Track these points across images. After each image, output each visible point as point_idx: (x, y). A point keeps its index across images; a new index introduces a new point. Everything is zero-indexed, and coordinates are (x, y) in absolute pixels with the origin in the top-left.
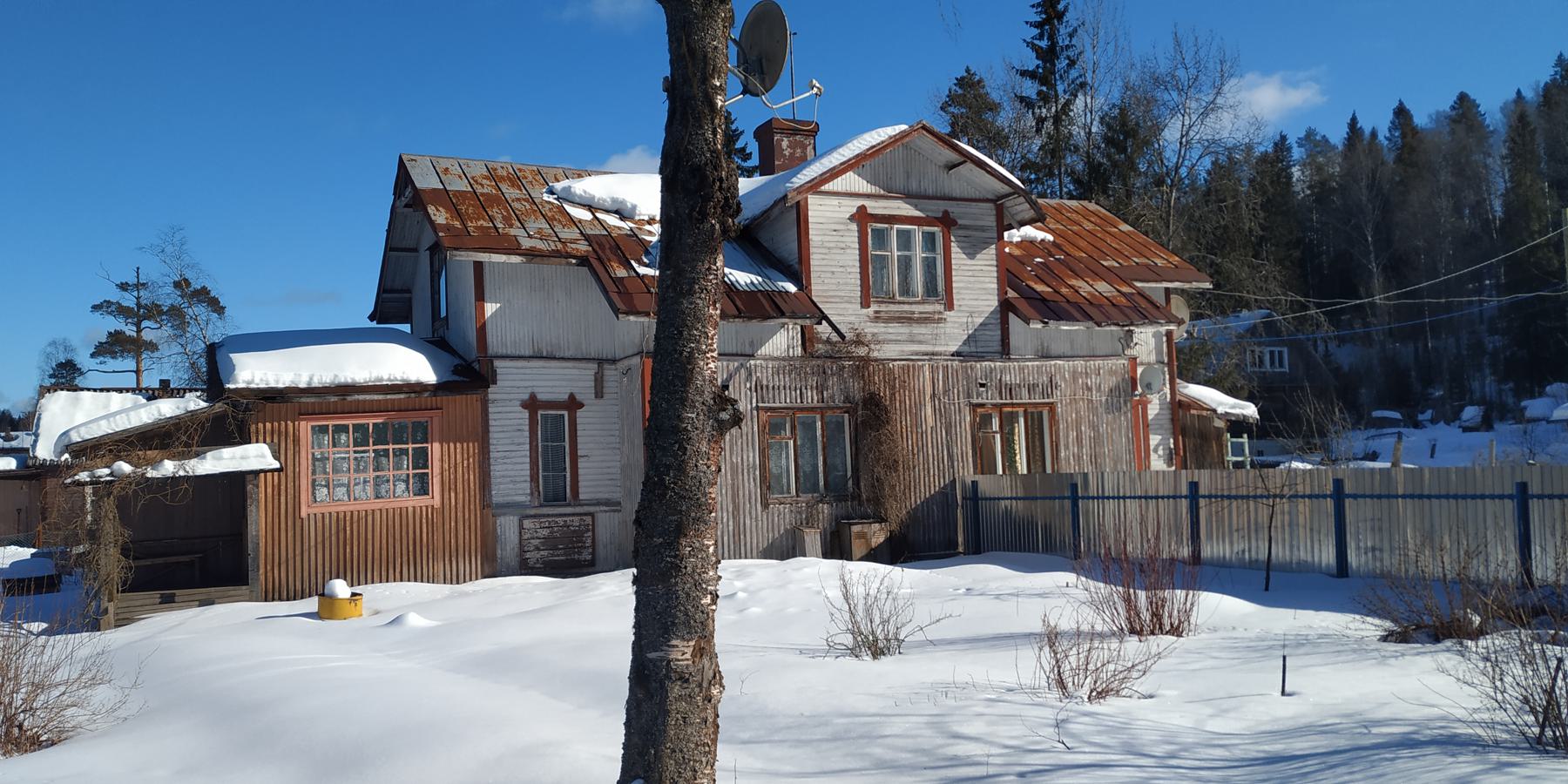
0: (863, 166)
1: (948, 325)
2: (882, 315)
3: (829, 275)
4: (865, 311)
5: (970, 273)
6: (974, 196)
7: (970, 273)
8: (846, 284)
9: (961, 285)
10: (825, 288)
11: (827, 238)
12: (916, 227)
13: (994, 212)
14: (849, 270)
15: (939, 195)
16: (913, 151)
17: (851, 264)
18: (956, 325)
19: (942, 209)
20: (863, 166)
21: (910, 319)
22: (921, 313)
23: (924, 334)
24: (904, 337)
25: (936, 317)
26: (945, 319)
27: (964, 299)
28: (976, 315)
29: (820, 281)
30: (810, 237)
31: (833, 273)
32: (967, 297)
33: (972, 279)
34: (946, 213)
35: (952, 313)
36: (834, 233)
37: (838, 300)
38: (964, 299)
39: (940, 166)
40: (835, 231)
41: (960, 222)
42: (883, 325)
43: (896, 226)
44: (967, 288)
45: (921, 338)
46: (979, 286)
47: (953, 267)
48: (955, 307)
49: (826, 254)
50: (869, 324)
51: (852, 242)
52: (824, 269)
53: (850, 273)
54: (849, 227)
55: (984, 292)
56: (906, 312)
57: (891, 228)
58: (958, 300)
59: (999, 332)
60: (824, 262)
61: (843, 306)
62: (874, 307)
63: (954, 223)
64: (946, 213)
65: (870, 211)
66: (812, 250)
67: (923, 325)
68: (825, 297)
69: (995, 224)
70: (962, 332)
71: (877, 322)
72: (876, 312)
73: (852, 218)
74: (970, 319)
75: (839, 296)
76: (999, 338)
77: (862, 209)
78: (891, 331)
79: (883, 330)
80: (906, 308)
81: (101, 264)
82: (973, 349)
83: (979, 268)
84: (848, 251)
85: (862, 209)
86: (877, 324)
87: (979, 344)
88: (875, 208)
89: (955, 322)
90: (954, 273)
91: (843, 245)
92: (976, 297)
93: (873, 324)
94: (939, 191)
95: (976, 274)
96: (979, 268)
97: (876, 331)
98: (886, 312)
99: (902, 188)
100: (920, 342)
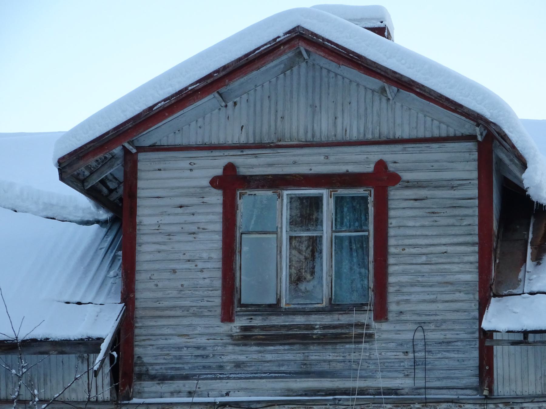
0: (235, 104)
1: (376, 345)
2: (256, 332)
3: (167, 275)
4: (226, 328)
5: (424, 259)
6: (436, 134)
7: (424, 259)
8: (196, 287)
9: (404, 279)
10: (160, 295)
11: (167, 219)
12: (324, 192)
13: (475, 155)
14: (201, 265)
15: (369, 137)
16: (324, 72)
17: (205, 255)
18: (392, 345)
19: (376, 158)
20: (235, 104)
21: (305, 337)
22: (325, 327)
23: (330, 361)
24: (293, 368)
25: (354, 331)
26: (370, 336)
27: (407, 301)
28: (432, 327)
29: (151, 285)
30: (138, 220)
31: (174, 271)
32: (413, 298)
33: (426, 268)
34: (381, 165)
35: (384, 326)
36: (180, 210)
37: (179, 313)
38: (407, 301)
39: (373, 91)
40: (181, 207)
41: (406, 176)
42: (255, 348)
43: (285, 193)
44: (412, 285)
45: (325, 367)
46: (439, 279)
47: (392, 250)
48: (391, 316)
49: (164, 243)
50: (230, 348)
51: (211, 222)
52: (157, 266)
53: (202, 271)
54: (205, 200)
55: (450, 288)
56: (298, 327)
57: (280, 196)
58: (398, 303)
59: (476, 354)
60: (159, 256)
61: (185, 321)
62: (240, 322)
63: (395, 179)
64: (381, 165)
65: (243, 171)
66: (140, 239)
67: (329, 347)
68: (157, 309)
69: (475, 175)
70: (401, 356)
71: (245, 345)
72: (245, 329)
73: (215, 182)
74: (419, 335)
75: (181, 307)
76: (476, 363)
77: (230, 168)
78: (269, 357)
79: (255, 356)
80: (299, 320)
81: (205, 278)
82: (420, 383)
83: (444, 249)
84: (201, 236)
85: (230, 168)
86: (244, 348)
87: (431, 375)
88: (253, 166)
89: (392, 341)
90: (391, 260)
91: (194, 228)
92: (432, 297)
93: (237, 348)
94: (318, 134)
95: (434, 260)
96: (444, 249)
97: (242, 358)
98: (263, 328)
99: (302, 131)
100: (321, 375)
